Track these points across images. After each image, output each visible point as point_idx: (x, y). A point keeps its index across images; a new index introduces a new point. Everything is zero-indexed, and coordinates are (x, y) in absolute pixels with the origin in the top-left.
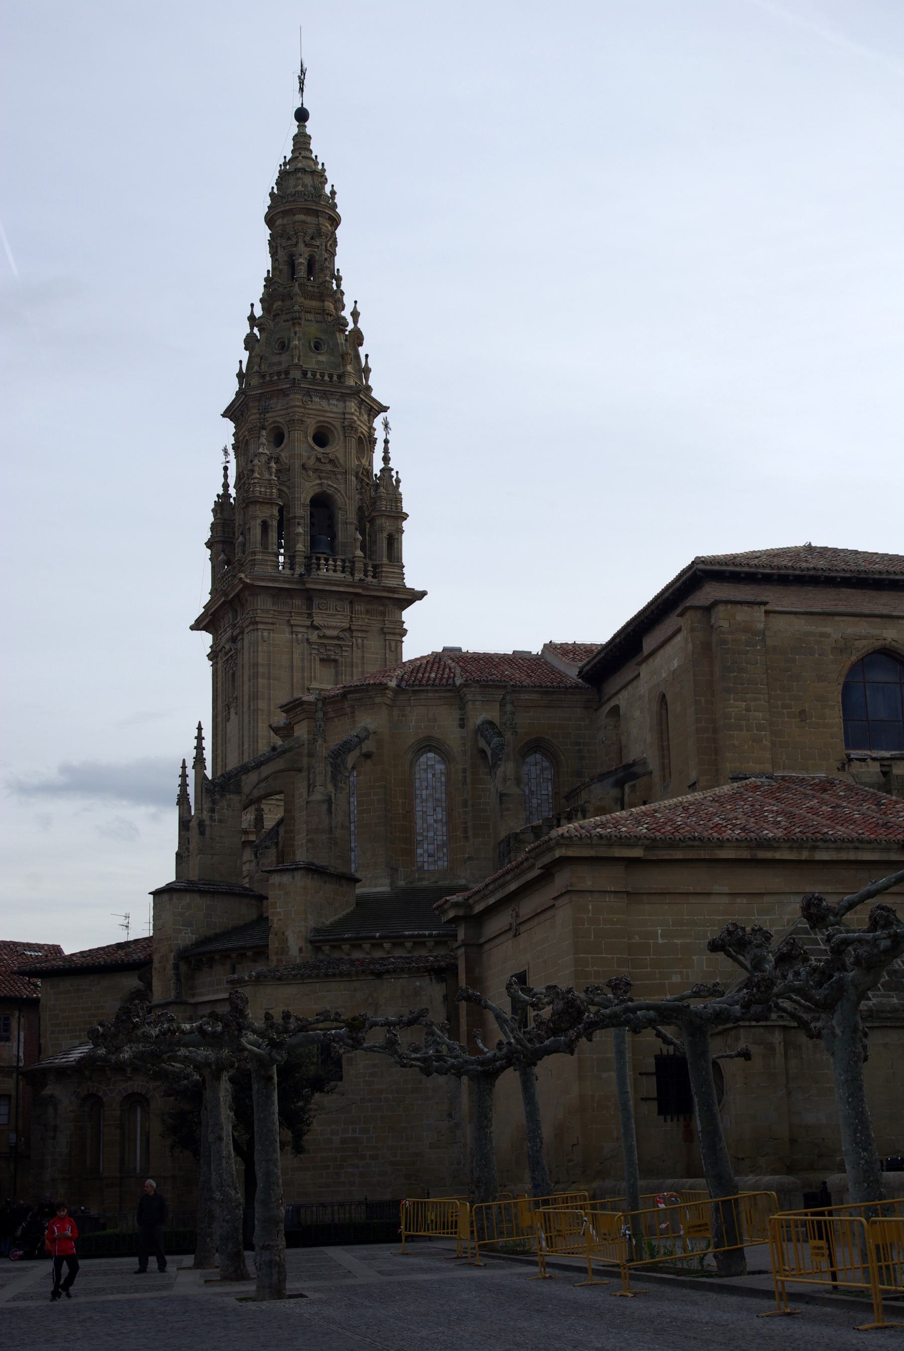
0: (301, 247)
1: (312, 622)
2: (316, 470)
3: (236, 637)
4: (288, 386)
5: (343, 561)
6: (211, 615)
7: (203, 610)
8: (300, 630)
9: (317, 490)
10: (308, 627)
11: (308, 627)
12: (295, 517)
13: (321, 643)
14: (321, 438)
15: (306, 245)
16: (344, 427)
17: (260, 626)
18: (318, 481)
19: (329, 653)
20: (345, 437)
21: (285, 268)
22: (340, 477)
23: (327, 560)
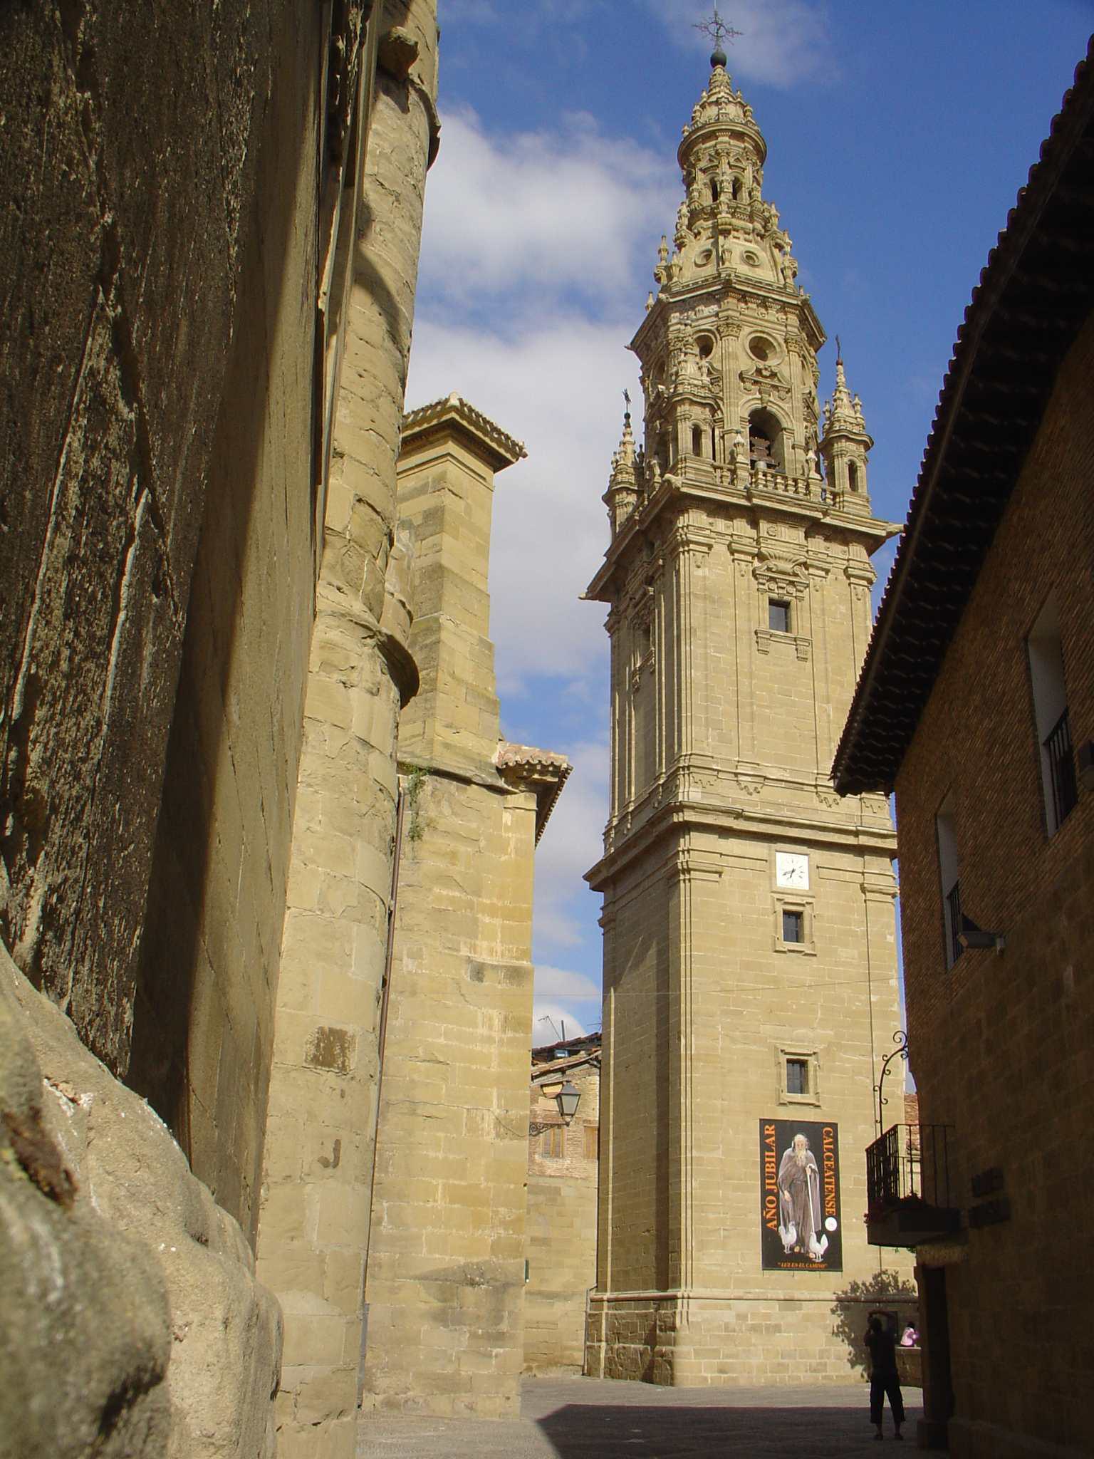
0: (725, 167)
1: (759, 549)
2: (756, 382)
3: (653, 577)
4: (719, 287)
5: (795, 481)
6: (615, 563)
7: (605, 559)
8: (742, 557)
9: (760, 406)
10: (753, 556)
11: (753, 556)
12: (730, 431)
13: (771, 577)
14: (760, 348)
15: (731, 166)
16: (786, 341)
17: (692, 546)
18: (758, 396)
19: (781, 591)
20: (789, 351)
21: (708, 193)
22: (783, 394)
23: (774, 476)
